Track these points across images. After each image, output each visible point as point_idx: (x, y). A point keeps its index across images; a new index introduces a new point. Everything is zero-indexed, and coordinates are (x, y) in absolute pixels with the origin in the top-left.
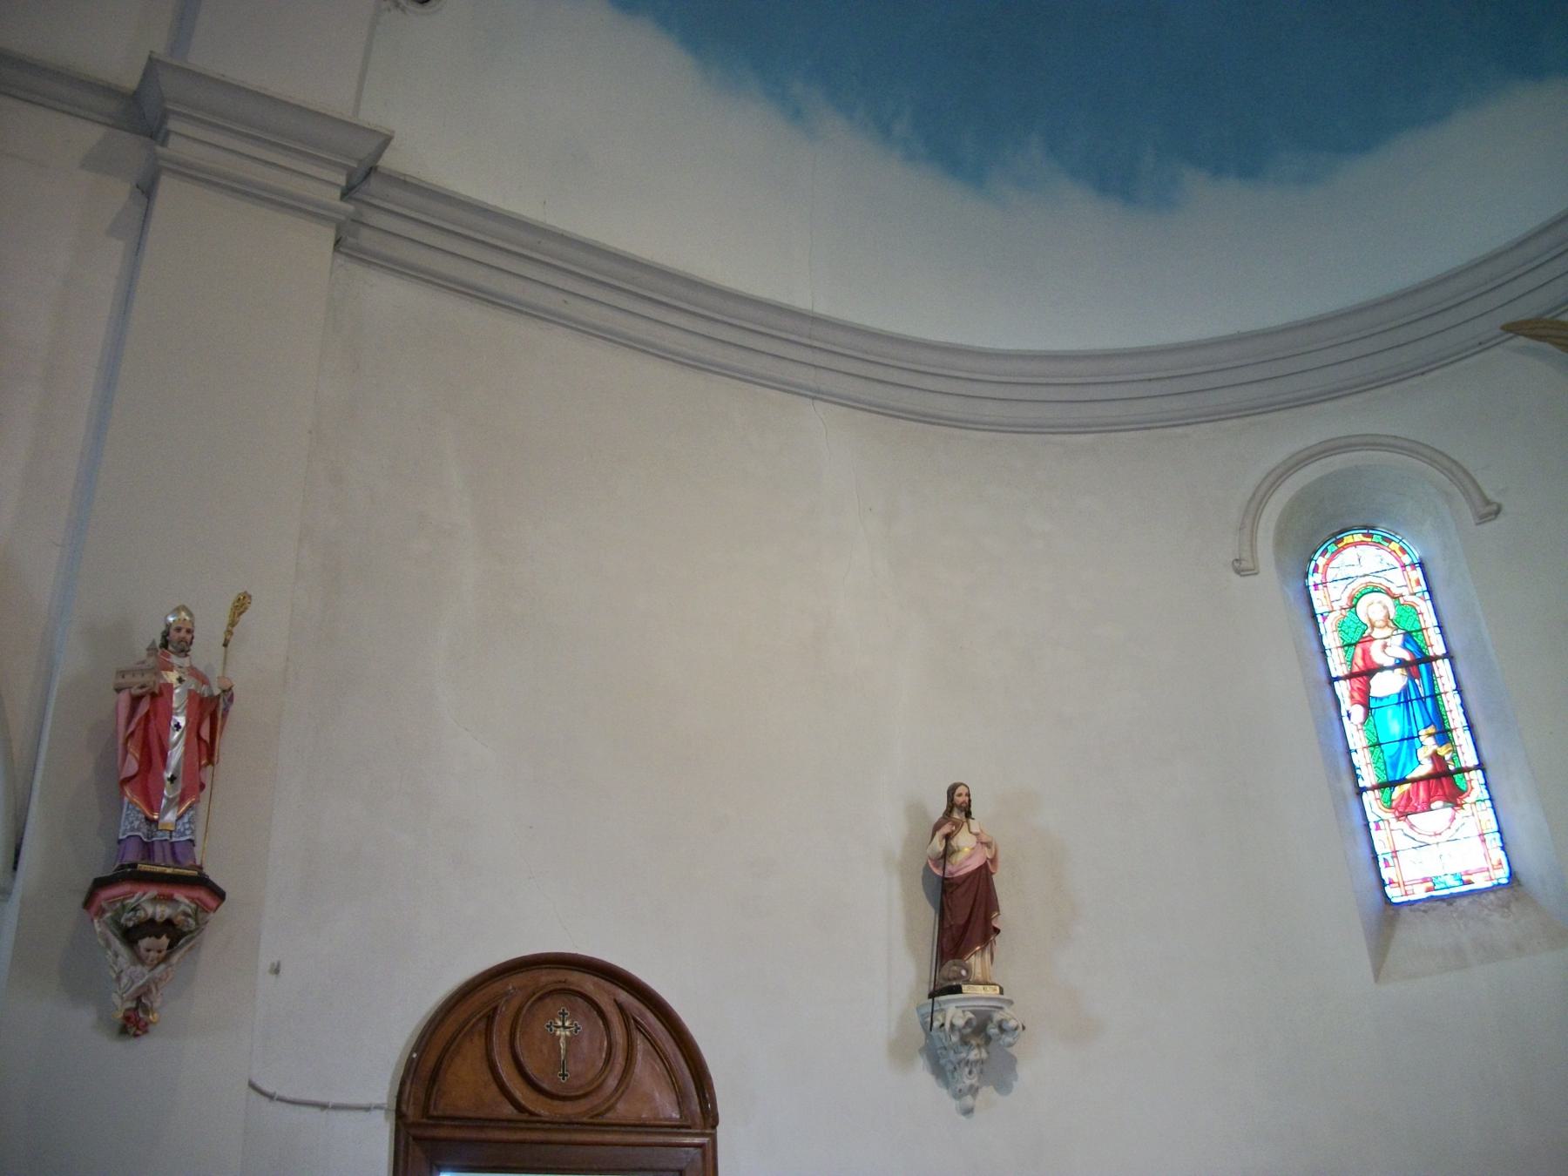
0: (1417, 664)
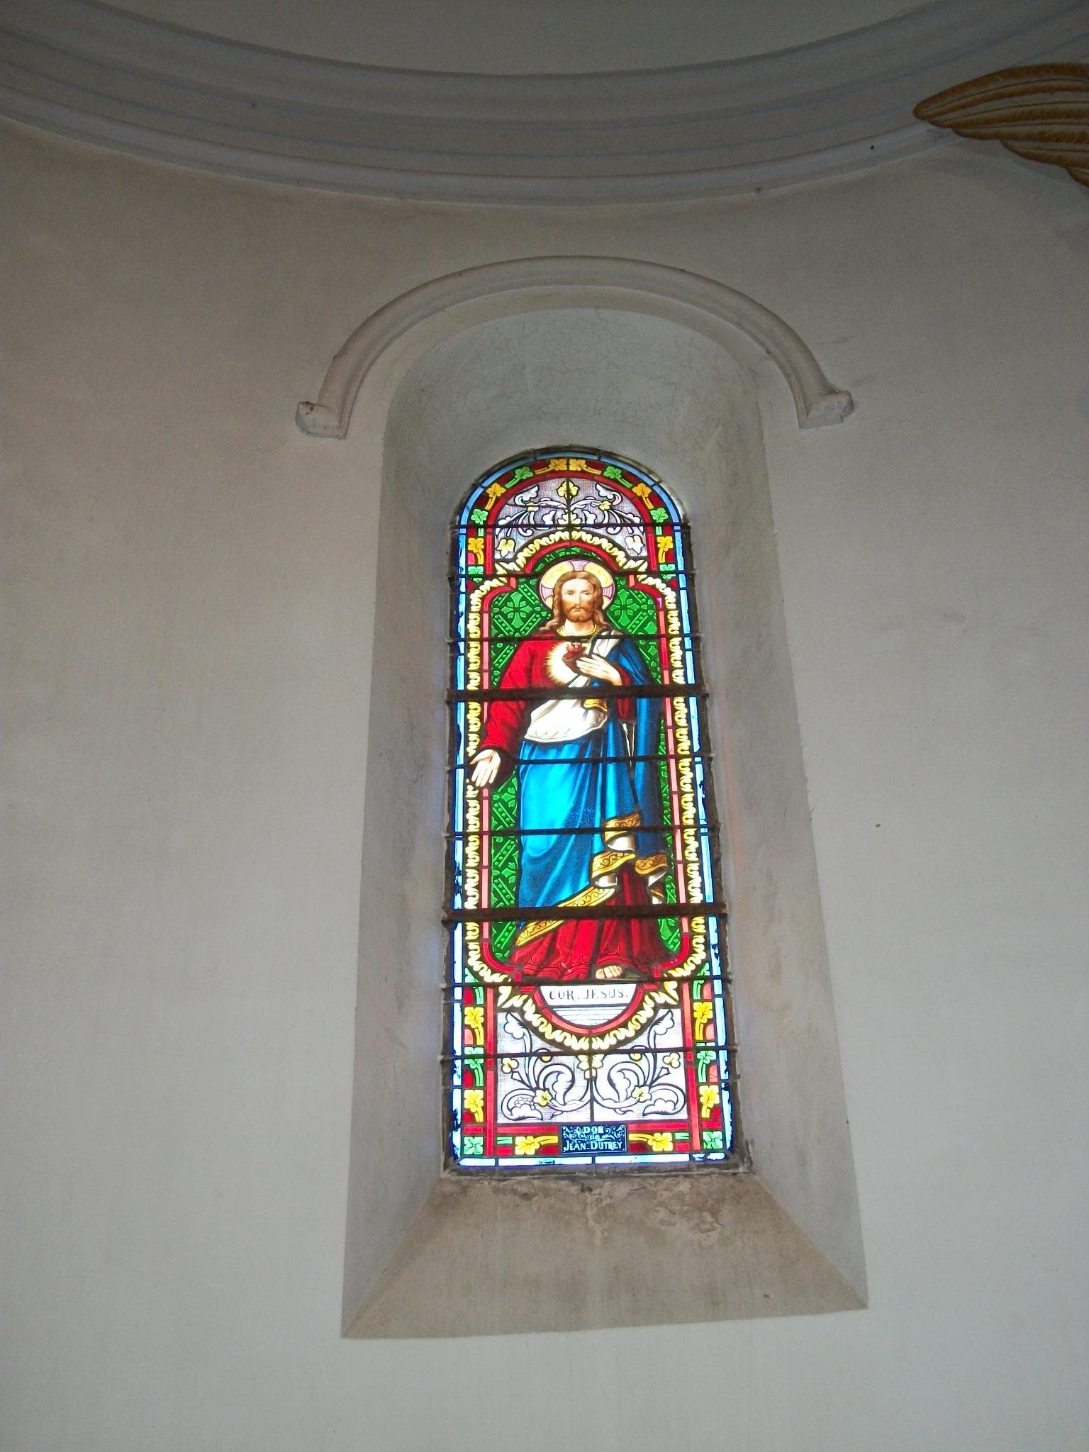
0: (634, 696)
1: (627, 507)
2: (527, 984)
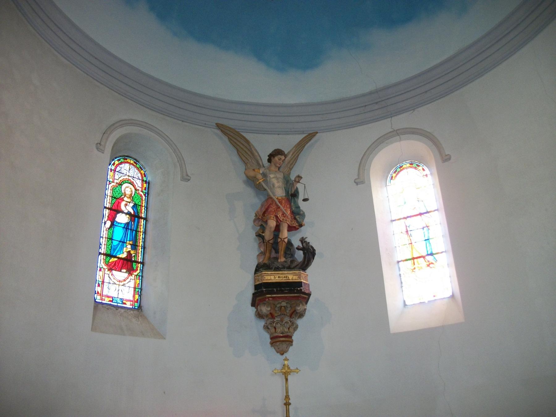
0: (134, 217)
1: (139, 175)
2: (110, 270)
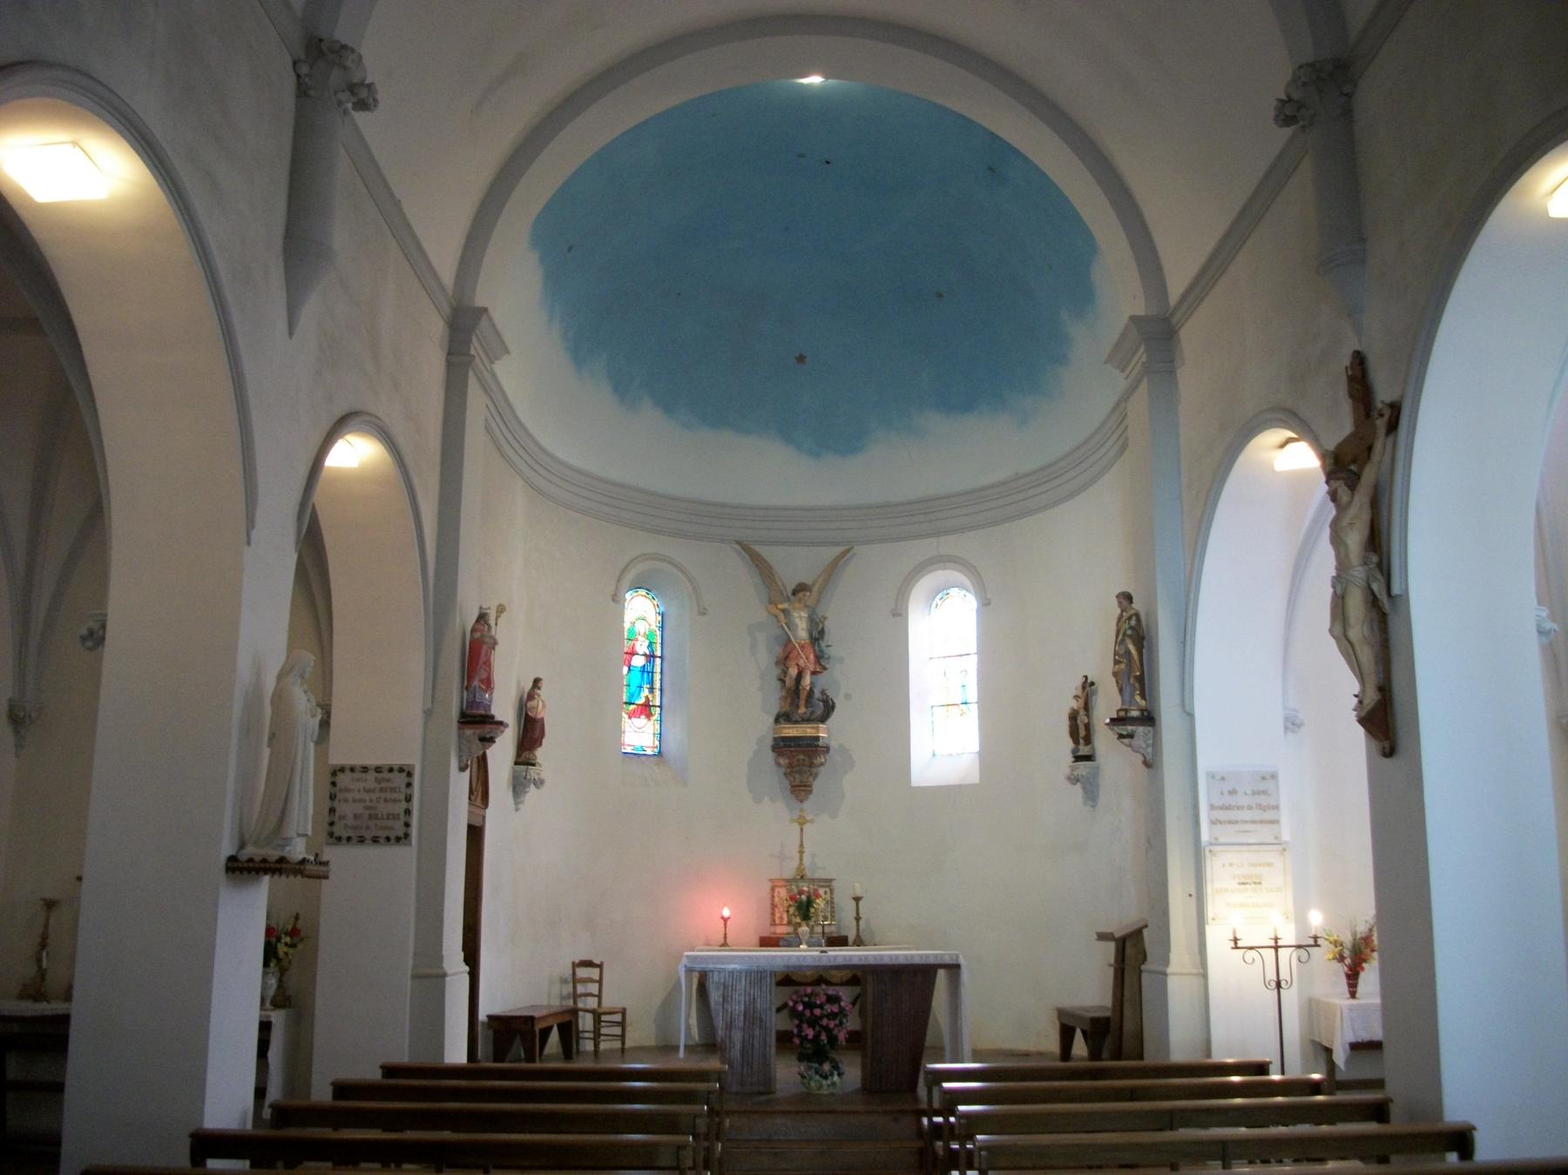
0: (650, 657)
